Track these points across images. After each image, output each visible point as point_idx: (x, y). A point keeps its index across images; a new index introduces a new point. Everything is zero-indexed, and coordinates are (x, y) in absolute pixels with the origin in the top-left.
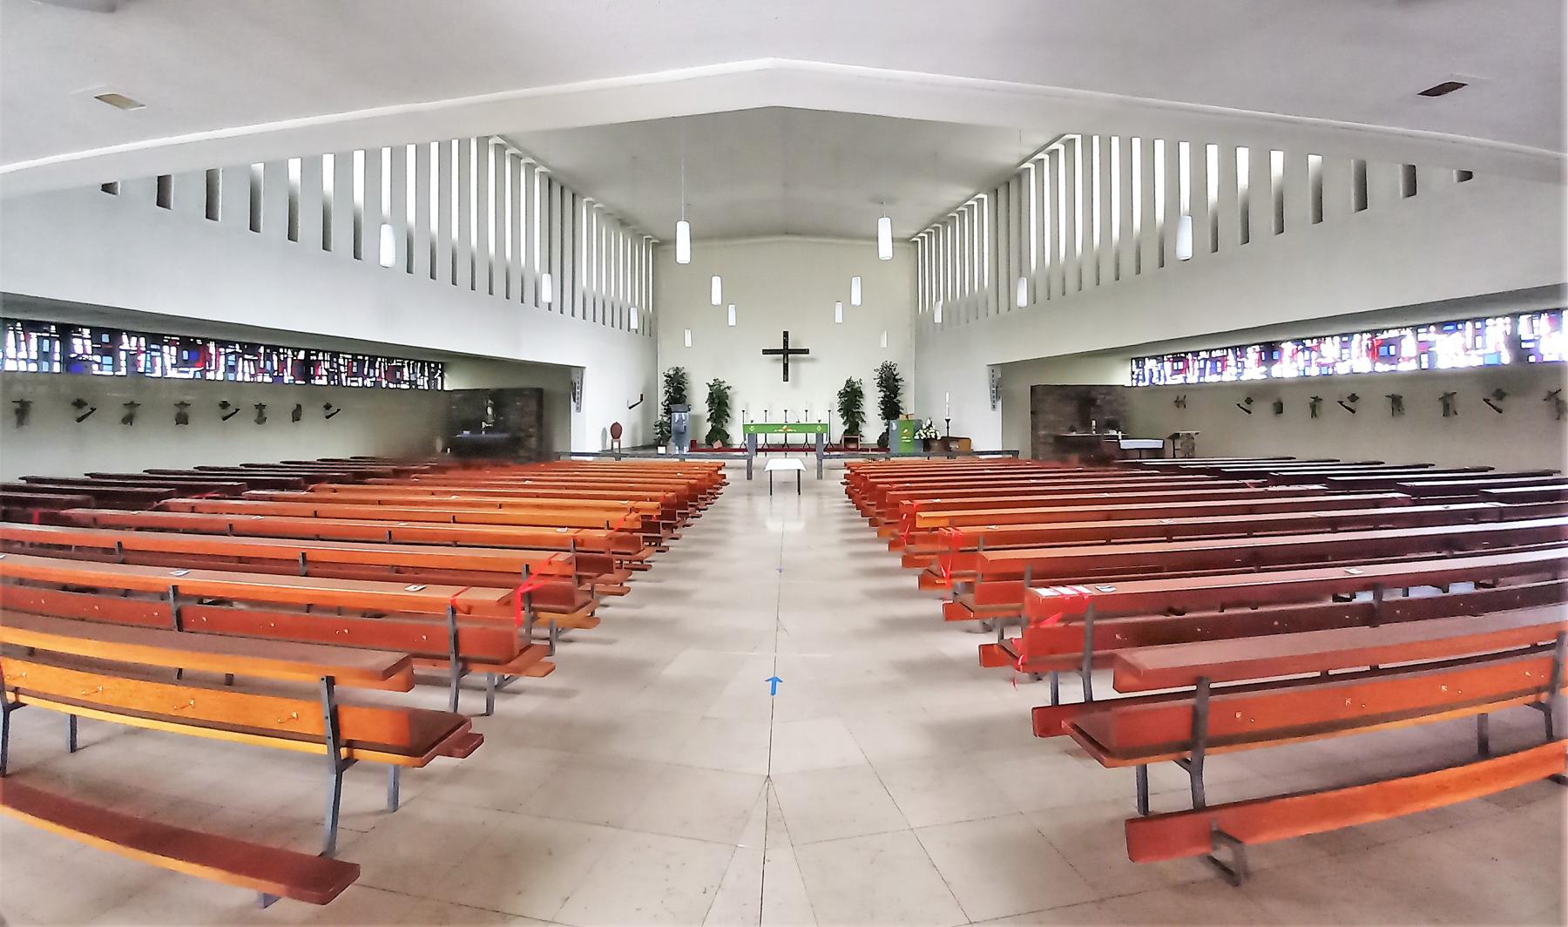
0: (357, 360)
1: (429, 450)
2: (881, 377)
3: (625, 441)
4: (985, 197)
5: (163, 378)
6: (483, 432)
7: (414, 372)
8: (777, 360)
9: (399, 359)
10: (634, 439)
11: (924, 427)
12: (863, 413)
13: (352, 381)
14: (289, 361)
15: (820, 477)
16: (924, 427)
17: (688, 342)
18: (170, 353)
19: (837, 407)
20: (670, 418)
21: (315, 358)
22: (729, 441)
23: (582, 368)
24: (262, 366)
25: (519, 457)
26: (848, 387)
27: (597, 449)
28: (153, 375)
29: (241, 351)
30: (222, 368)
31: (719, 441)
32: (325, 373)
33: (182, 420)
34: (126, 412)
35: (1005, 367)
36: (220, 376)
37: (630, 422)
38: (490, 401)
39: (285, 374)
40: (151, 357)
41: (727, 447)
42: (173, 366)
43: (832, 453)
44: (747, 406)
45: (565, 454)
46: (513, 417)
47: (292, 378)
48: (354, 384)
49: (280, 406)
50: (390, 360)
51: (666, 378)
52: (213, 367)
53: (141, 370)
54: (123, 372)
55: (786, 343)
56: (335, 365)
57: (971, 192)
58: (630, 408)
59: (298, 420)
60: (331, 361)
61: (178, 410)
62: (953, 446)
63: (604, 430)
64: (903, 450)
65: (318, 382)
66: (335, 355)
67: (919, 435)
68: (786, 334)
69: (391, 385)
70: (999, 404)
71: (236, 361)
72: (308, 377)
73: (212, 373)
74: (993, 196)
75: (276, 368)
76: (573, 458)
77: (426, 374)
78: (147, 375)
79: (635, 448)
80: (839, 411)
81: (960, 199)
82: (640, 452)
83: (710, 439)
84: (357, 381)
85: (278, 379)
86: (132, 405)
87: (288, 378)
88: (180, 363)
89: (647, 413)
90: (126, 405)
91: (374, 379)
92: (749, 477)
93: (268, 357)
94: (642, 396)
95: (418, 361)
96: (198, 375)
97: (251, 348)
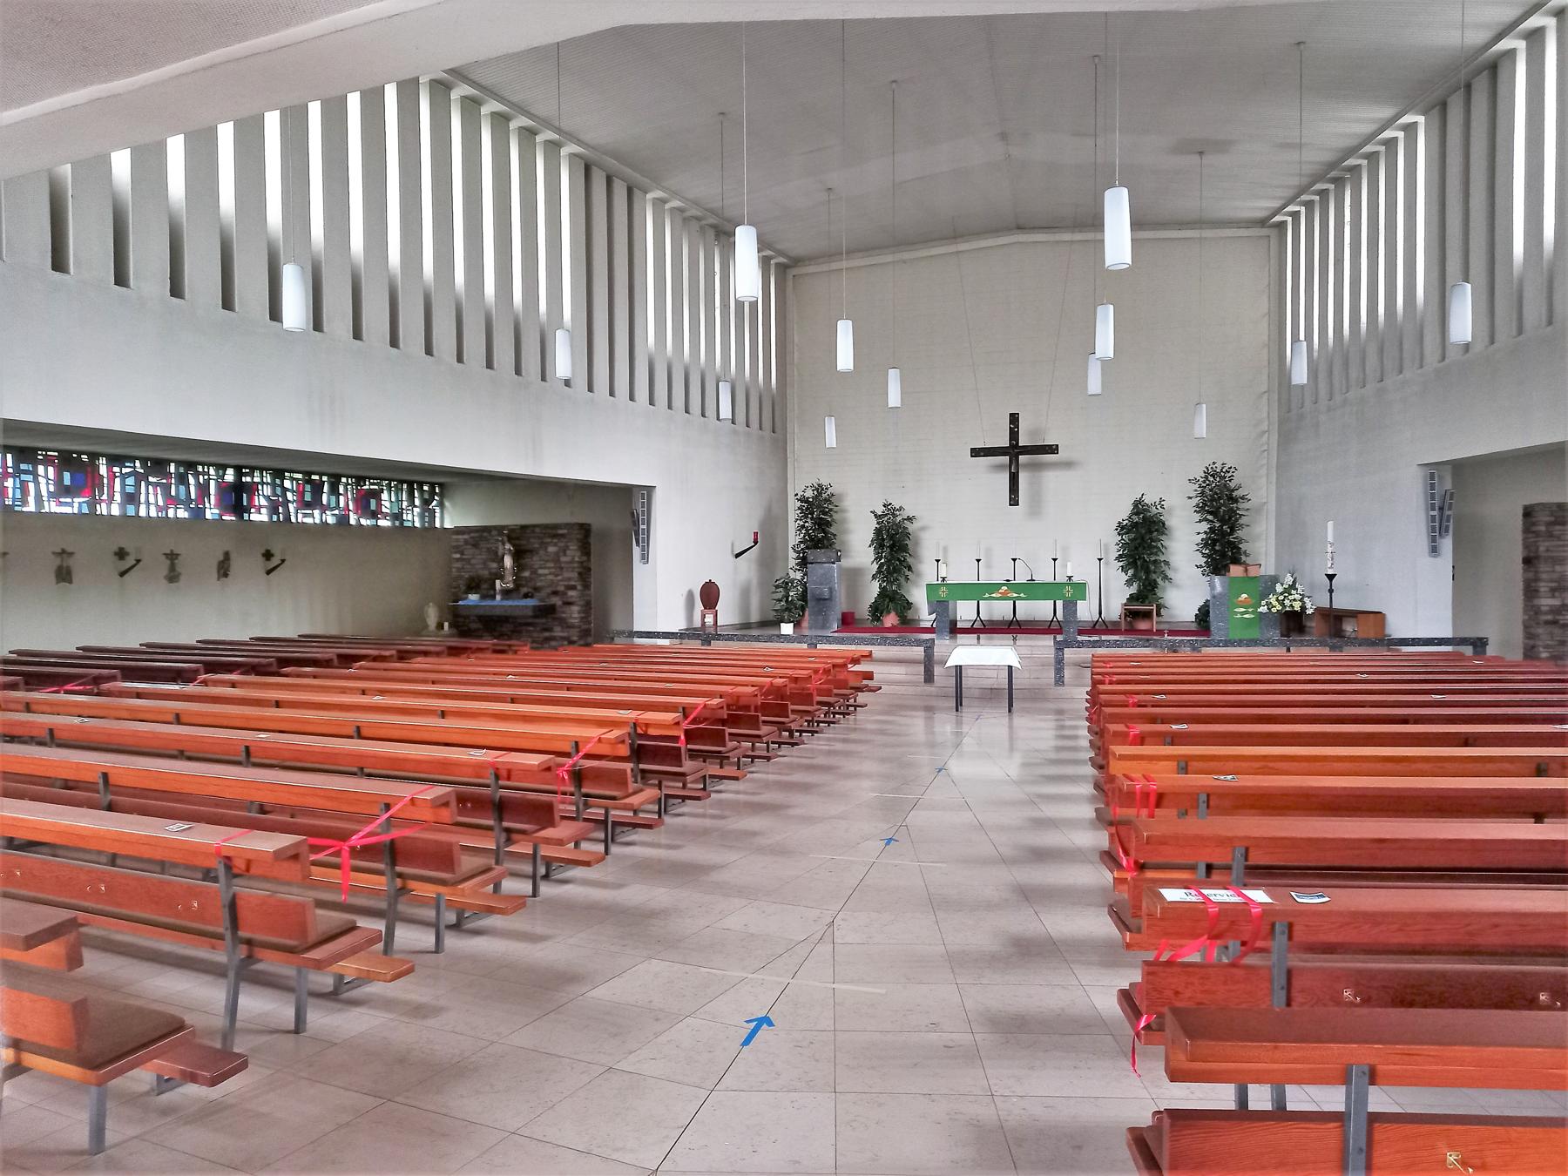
0: (309, 481)
1: (419, 628)
2: (1203, 492)
3: (727, 613)
4: (1421, 119)
5: (39, 514)
6: (498, 597)
7: (397, 500)
8: (999, 467)
10: (745, 606)
11: (1279, 588)
12: (1167, 563)
13: (305, 515)
14: (212, 483)
15: (1060, 681)
16: (1279, 588)
17: (831, 439)
18: (46, 473)
19: (1114, 552)
21: (248, 479)
22: (910, 615)
24: (173, 493)
26: (1137, 514)
27: (677, 624)
28: (25, 509)
29: (142, 471)
30: (118, 497)
31: (893, 614)
32: (263, 502)
33: (64, 575)
35: (1459, 468)
36: (115, 510)
37: (734, 578)
38: (508, 546)
39: (207, 505)
41: (908, 624)
42: (51, 495)
43: (1104, 638)
44: (945, 549)
45: (620, 633)
46: (544, 572)
47: (217, 511)
48: (309, 520)
49: (200, 555)
50: (360, 480)
51: (799, 504)
52: (105, 497)
53: (9, 502)
55: (1014, 435)
56: (279, 491)
57: (1386, 112)
58: (738, 556)
59: (226, 575)
60: (274, 485)
61: (58, 561)
62: (1349, 627)
63: (690, 595)
64: (1235, 635)
65: (255, 517)
66: (279, 474)
68: (1014, 419)
69: (363, 522)
70: (1447, 544)
71: (137, 486)
72: (239, 509)
73: (104, 505)
74: (1436, 112)
75: (193, 497)
76: (638, 641)
77: (417, 502)
78: (17, 509)
79: (746, 626)
80: (1119, 558)
81: (1367, 129)
82: (755, 633)
83: (877, 610)
84: (312, 515)
85: (198, 513)
87: (211, 513)
88: (62, 491)
89: (767, 563)
90: (54, 553)
91: (336, 512)
92: (929, 678)
93: (182, 480)
94: (756, 534)
95: (401, 482)
96: (85, 510)
97: (158, 466)
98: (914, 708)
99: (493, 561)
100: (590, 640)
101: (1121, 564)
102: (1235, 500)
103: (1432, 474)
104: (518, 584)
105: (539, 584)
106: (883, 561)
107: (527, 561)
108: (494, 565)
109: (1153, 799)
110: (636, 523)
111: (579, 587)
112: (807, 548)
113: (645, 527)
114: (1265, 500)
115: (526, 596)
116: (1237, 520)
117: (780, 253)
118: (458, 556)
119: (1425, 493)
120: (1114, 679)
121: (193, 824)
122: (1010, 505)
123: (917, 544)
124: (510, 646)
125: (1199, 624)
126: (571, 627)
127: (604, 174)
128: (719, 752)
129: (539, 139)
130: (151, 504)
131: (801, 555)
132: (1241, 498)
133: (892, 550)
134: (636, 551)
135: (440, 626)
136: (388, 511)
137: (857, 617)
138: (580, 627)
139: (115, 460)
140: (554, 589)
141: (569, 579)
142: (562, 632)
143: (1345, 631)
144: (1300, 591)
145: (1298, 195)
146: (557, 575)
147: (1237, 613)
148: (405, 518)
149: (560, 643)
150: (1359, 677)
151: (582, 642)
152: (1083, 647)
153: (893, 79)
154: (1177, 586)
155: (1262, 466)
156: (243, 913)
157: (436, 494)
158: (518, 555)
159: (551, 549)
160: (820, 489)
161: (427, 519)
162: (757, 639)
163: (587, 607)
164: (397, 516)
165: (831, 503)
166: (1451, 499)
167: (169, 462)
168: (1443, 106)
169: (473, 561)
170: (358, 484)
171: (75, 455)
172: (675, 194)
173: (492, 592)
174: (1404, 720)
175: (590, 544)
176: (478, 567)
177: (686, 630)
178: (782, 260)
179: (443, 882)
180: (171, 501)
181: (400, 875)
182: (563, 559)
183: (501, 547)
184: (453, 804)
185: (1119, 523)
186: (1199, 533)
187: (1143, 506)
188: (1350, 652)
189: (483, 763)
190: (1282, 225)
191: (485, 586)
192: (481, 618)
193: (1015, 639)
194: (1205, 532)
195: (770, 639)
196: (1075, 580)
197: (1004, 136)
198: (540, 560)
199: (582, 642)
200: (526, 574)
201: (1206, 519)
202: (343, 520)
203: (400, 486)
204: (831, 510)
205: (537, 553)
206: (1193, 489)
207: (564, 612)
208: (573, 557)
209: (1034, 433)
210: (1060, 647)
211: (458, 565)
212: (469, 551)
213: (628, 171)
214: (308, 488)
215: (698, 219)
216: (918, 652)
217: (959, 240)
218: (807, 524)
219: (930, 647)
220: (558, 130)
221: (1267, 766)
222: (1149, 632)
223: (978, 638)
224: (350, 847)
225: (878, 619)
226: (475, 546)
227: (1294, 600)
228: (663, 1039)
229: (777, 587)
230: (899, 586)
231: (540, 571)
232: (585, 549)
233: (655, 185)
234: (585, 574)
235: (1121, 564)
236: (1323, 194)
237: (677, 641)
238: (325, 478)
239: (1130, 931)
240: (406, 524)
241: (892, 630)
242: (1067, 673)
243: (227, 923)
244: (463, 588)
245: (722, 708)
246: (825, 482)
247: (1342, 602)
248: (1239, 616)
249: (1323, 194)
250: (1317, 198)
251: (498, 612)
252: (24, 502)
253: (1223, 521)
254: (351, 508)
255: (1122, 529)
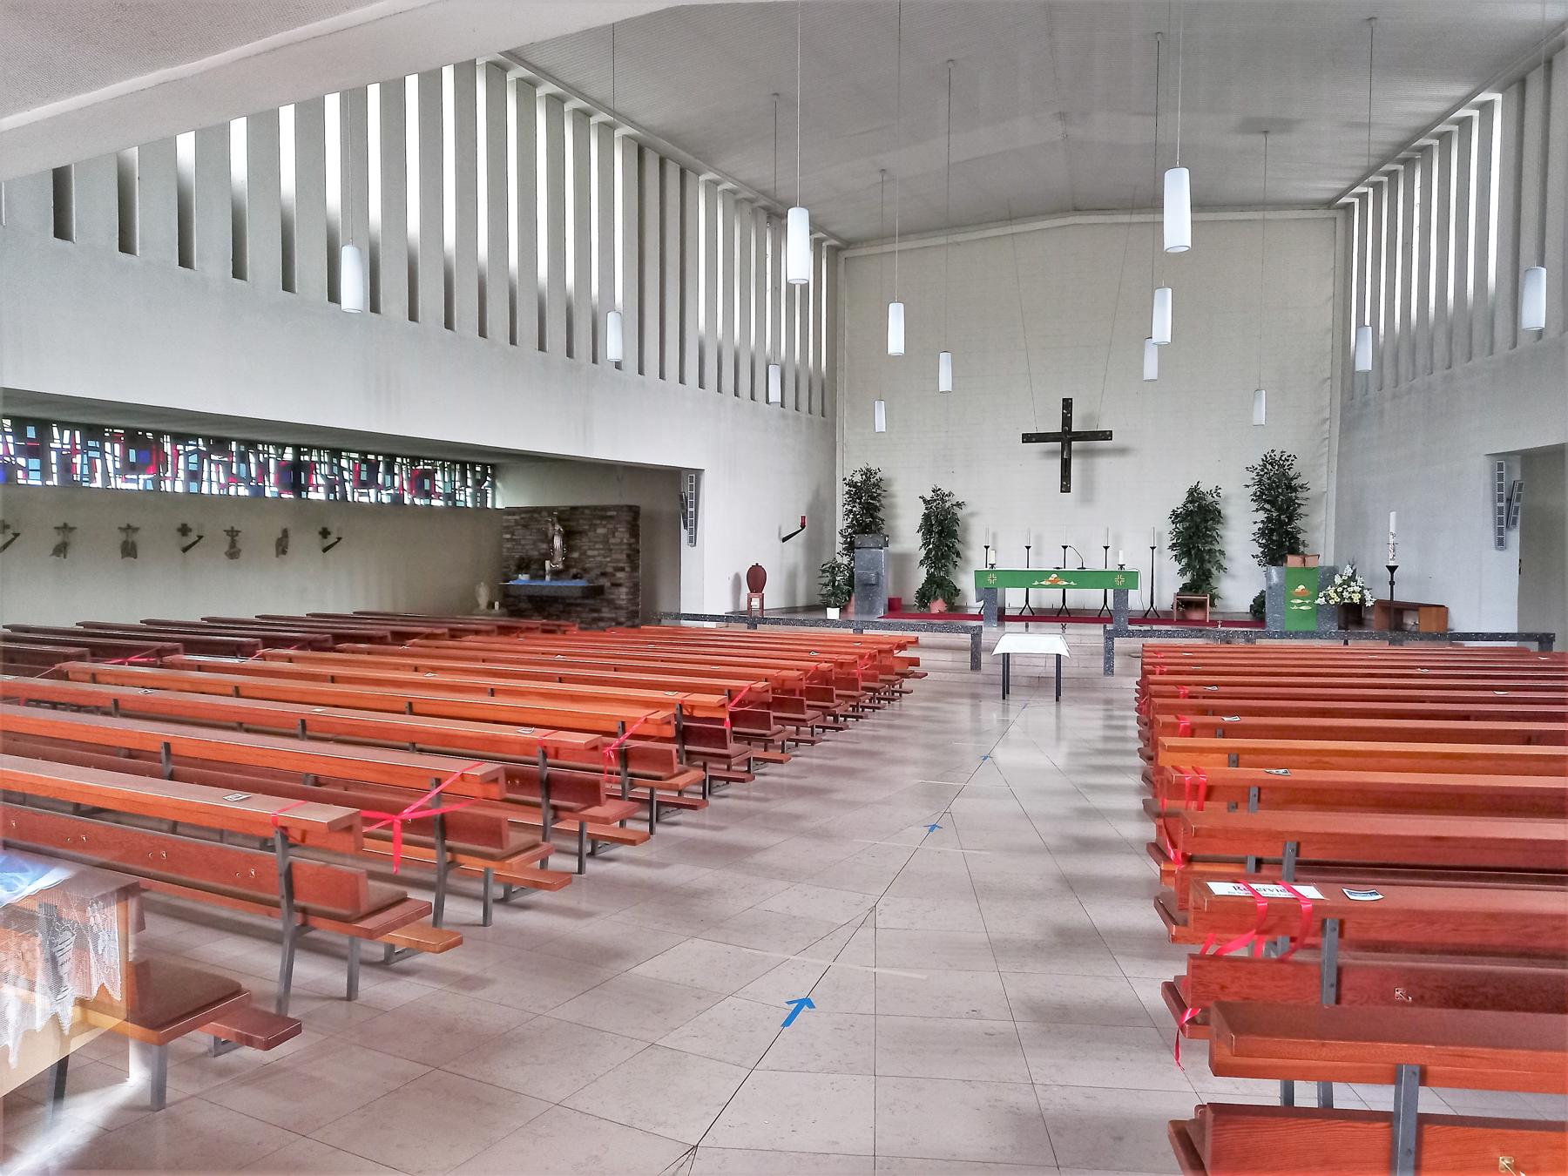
0: (366, 461)
2: (1260, 481)
3: (773, 597)
4: (1498, 97)
5: (105, 490)
6: (548, 578)
8: (1052, 453)
9: (428, 460)
10: (791, 592)
11: (1338, 580)
12: (1222, 553)
13: (361, 494)
14: (272, 463)
15: (1109, 670)
16: (1338, 580)
17: (881, 423)
18: (114, 450)
20: (853, 559)
21: (307, 458)
22: (957, 601)
23: (698, 472)
24: (234, 471)
25: (602, 619)
26: (1191, 502)
27: (724, 607)
28: (92, 485)
29: (204, 449)
30: (181, 474)
31: (940, 600)
32: (321, 481)
33: (129, 550)
34: (58, 539)
35: (1528, 457)
36: (179, 488)
37: (781, 563)
39: (267, 483)
40: (90, 459)
41: (955, 611)
43: (1155, 627)
44: (995, 536)
45: (668, 615)
46: (594, 554)
47: (276, 489)
48: (364, 499)
50: (415, 460)
51: (847, 488)
54: (54, 481)
55: (1067, 420)
56: (335, 469)
57: (1460, 90)
58: (784, 540)
59: (284, 552)
60: (331, 464)
61: (122, 537)
62: (1410, 621)
63: (737, 578)
64: (1291, 626)
65: (312, 496)
66: (336, 453)
67: (1327, 597)
68: (1067, 404)
69: (417, 501)
70: (1514, 537)
72: (298, 487)
73: (168, 482)
74: (1514, 89)
75: (253, 475)
76: (684, 623)
77: (470, 482)
78: (84, 484)
79: (792, 610)
80: (1172, 547)
81: (1439, 107)
82: (801, 617)
83: (924, 597)
85: (258, 492)
86: (65, 528)
88: (129, 468)
90: (120, 528)
91: (391, 491)
92: (976, 665)
93: (243, 458)
94: (803, 518)
95: (454, 462)
96: (150, 487)
97: (220, 444)
98: (960, 695)
99: (543, 541)
100: (637, 621)
101: (1175, 553)
102: (1295, 490)
103: (1500, 467)
104: (567, 566)
105: (588, 565)
106: (931, 546)
107: (577, 542)
108: (544, 546)
109: (1202, 792)
110: (684, 506)
111: (627, 569)
112: (854, 532)
113: (693, 510)
114: (1325, 490)
115: (575, 577)
116: (1295, 510)
117: (833, 235)
118: (508, 536)
119: (1494, 484)
120: (1165, 670)
121: (251, 795)
122: (1062, 492)
123: (966, 530)
124: (559, 626)
125: (1254, 615)
126: (619, 608)
127: (657, 156)
128: (764, 735)
129: (593, 120)
130: (214, 481)
131: (849, 540)
132: (1301, 488)
133: (940, 536)
134: (684, 534)
135: (491, 605)
136: (441, 491)
137: (903, 603)
138: (627, 608)
139: (179, 438)
140: (603, 571)
141: (618, 561)
142: (610, 612)
143: (1406, 624)
144: (1359, 583)
145: (1366, 176)
146: (605, 557)
147: (1293, 605)
148: (457, 498)
149: (608, 624)
150: (1419, 671)
151: (629, 623)
152: (1133, 636)
153: (951, 58)
154: (1233, 577)
155: (1324, 454)
156: (299, 883)
157: (488, 474)
158: (568, 536)
159: (601, 531)
160: (868, 473)
161: (479, 499)
162: (803, 623)
163: (635, 589)
164: (450, 497)
165: (879, 488)
166: (1520, 489)
167: (230, 440)
168: (1523, 82)
169: (523, 542)
170: (412, 463)
171: (140, 433)
172: (728, 176)
173: (541, 573)
174: (1466, 717)
175: (638, 527)
176: (527, 547)
177: (733, 613)
178: (833, 242)
179: (491, 857)
180: (233, 479)
181: (450, 849)
182: (612, 541)
183: (551, 528)
184: (502, 780)
185: (1174, 511)
186: (1255, 523)
187: (1198, 494)
188: (1412, 646)
189: (531, 741)
190: (1350, 206)
191: (534, 566)
192: (531, 598)
193: (1064, 627)
194: (1262, 522)
195: (816, 623)
196: (1126, 568)
197: (1062, 116)
198: (590, 542)
199: (629, 623)
200: (575, 555)
201: (1263, 509)
202: (397, 500)
203: (453, 467)
204: (879, 495)
205: (587, 535)
206: (1250, 477)
207: (612, 594)
208: (622, 540)
209: (1089, 417)
210: (1109, 637)
211: (509, 545)
212: (520, 532)
213: (682, 153)
214: (364, 467)
215: (751, 201)
216: (965, 639)
217: (1014, 221)
218: (854, 509)
219: (977, 634)
220: (613, 112)
221: (1320, 760)
222: (1202, 622)
223: (1027, 626)
224: (401, 820)
225: (925, 606)
226: (525, 526)
227: (1354, 592)
228: (704, 1017)
229: (824, 571)
230: (947, 572)
231: (590, 553)
232: (634, 531)
233: (708, 167)
234: (633, 556)
235: (1175, 553)
236: (1392, 175)
237: (723, 624)
238: (380, 458)
239: (1176, 924)
240: (459, 504)
241: (940, 616)
242: (1117, 663)
243: (284, 891)
244: (513, 568)
245: (767, 691)
246: (874, 468)
247: (1403, 595)
248: (1295, 607)
249: (1392, 175)
250: (1385, 179)
251: (545, 592)
252: (92, 479)
253: (1280, 510)
254: (405, 487)
255: (1176, 517)
